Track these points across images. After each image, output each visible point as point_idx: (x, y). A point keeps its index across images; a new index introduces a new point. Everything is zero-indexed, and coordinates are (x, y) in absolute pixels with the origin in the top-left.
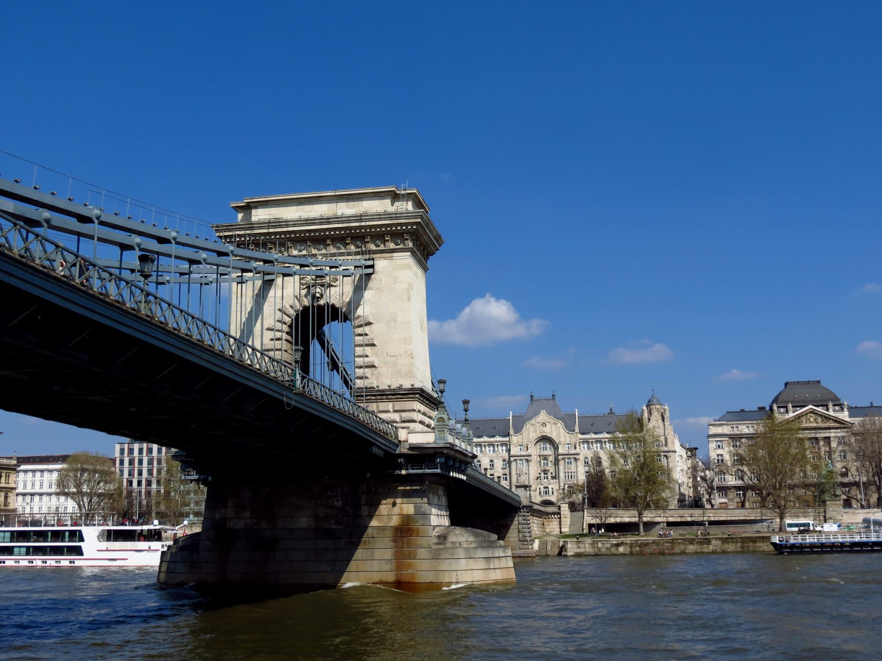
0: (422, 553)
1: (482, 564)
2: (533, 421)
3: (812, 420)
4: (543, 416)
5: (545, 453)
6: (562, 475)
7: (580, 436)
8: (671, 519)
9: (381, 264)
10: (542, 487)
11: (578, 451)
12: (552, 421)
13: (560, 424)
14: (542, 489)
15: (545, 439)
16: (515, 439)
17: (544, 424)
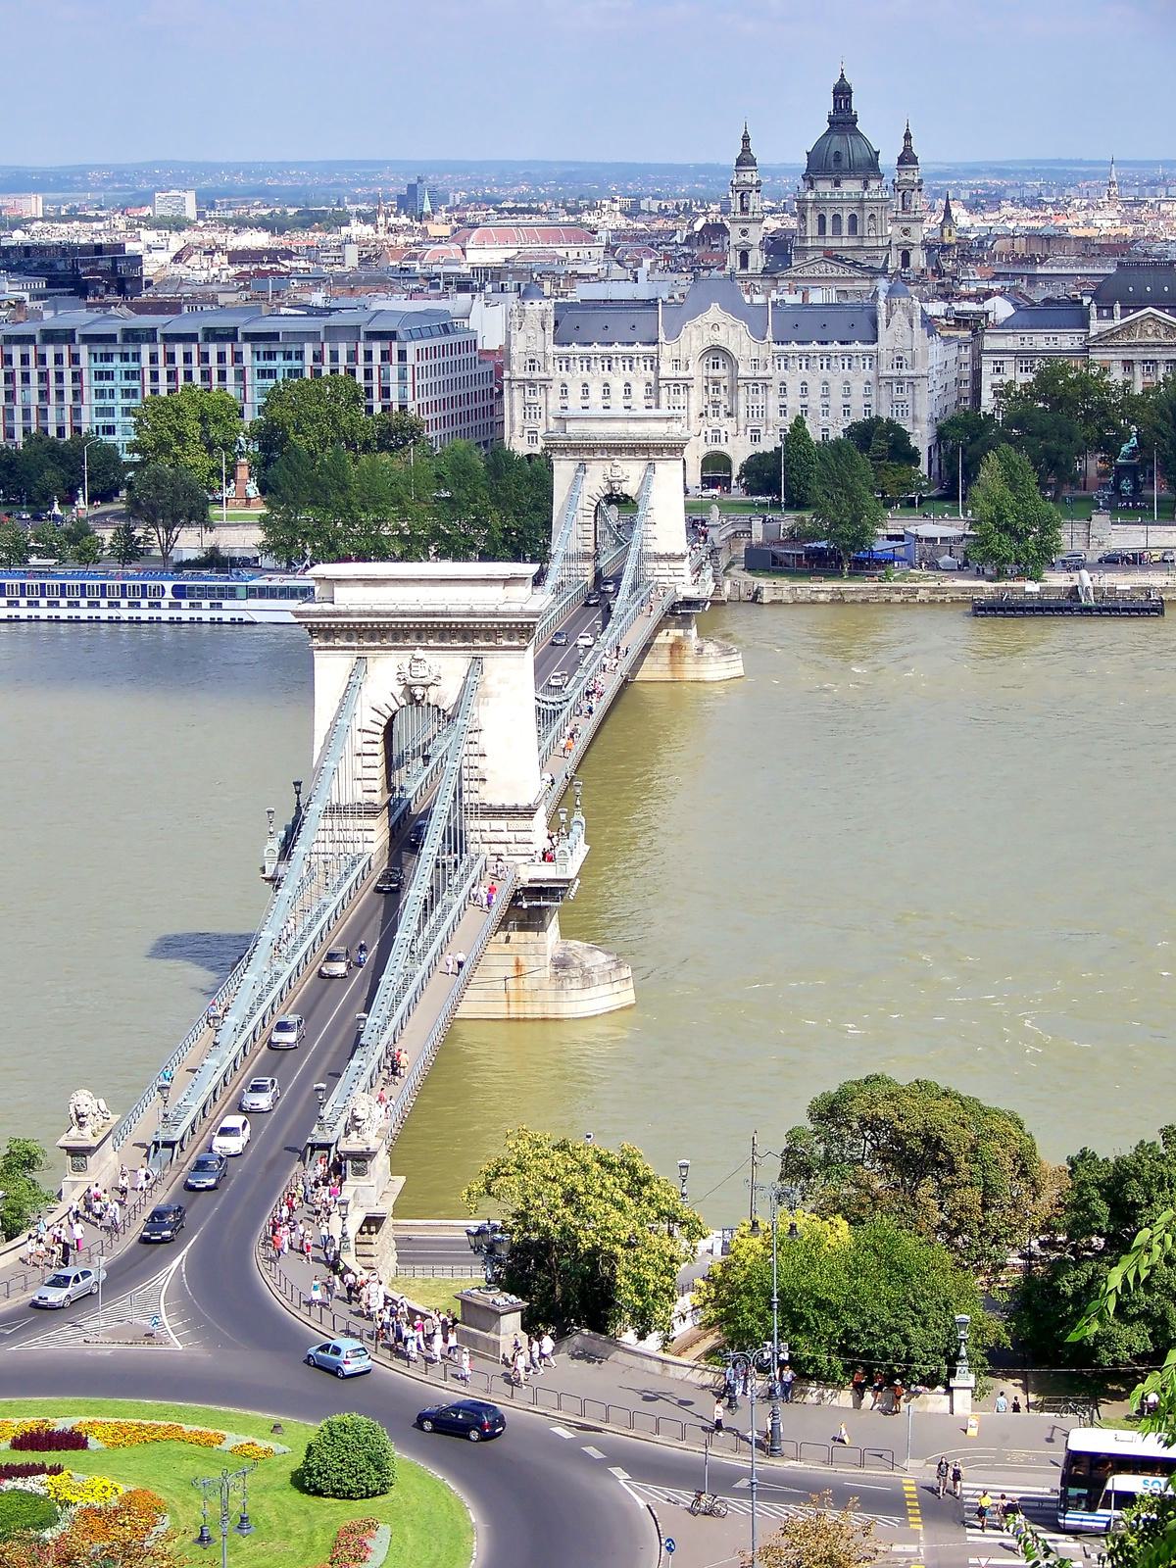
0: (688, 660)
1: (725, 666)
2: (698, 321)
3: (1150, 332)
4: (714, 313)
5: (716, 373)
6: (742, 411)
7: (775, 347)
8: (893, 532)
9: (659, 466)
10: (709, 430)
11: (769, 372)
12: (731, 322)
13: (742, 326)
14: (710, 433)
15: (717, 354)
16: (667, 351)
17: (715, 326)
